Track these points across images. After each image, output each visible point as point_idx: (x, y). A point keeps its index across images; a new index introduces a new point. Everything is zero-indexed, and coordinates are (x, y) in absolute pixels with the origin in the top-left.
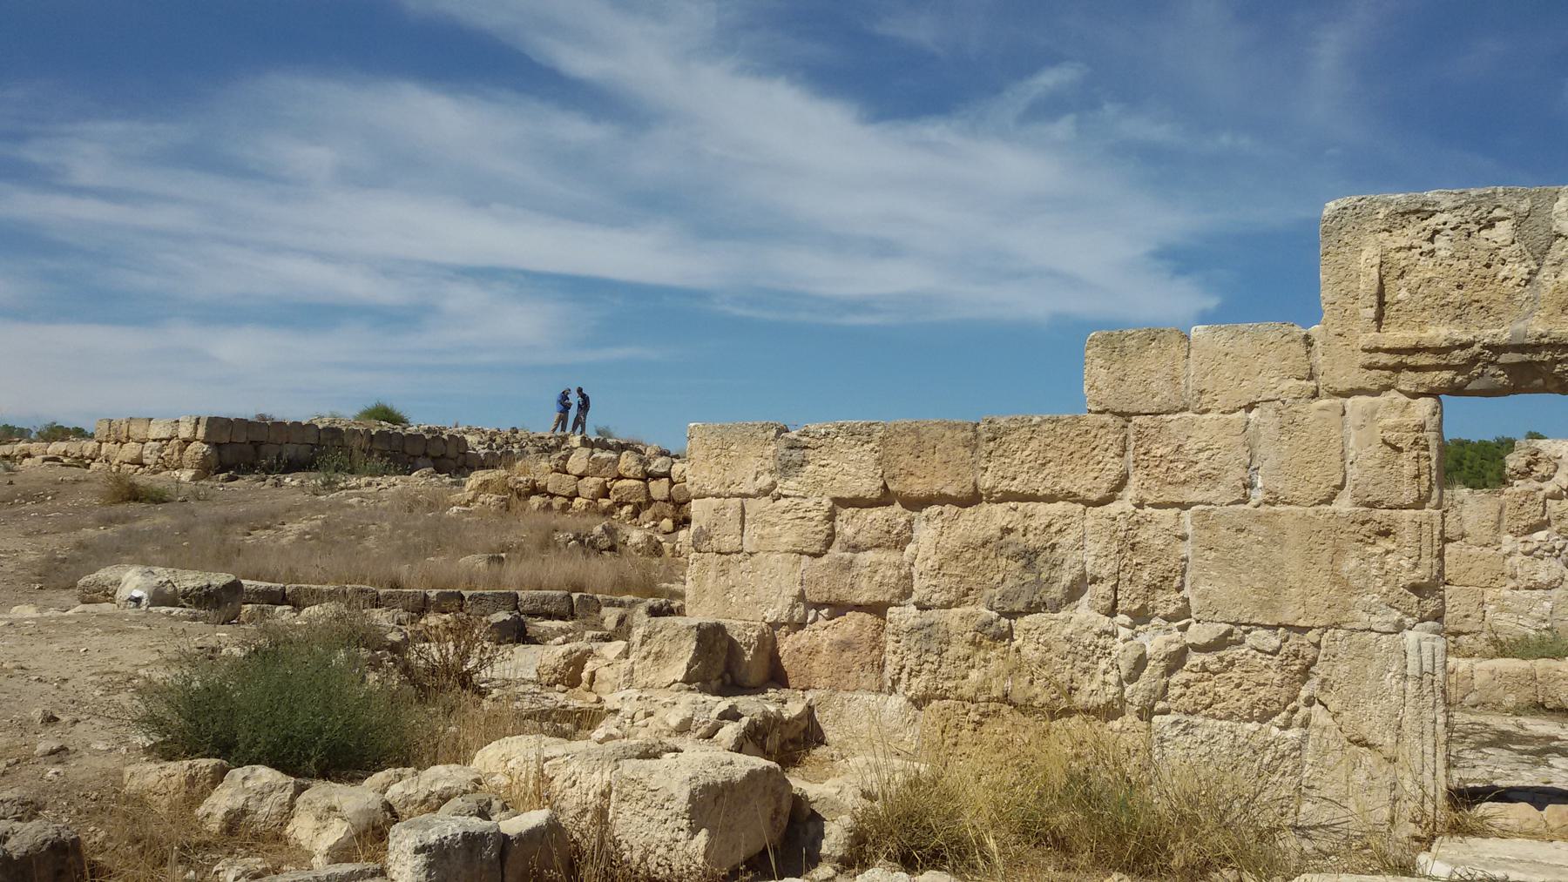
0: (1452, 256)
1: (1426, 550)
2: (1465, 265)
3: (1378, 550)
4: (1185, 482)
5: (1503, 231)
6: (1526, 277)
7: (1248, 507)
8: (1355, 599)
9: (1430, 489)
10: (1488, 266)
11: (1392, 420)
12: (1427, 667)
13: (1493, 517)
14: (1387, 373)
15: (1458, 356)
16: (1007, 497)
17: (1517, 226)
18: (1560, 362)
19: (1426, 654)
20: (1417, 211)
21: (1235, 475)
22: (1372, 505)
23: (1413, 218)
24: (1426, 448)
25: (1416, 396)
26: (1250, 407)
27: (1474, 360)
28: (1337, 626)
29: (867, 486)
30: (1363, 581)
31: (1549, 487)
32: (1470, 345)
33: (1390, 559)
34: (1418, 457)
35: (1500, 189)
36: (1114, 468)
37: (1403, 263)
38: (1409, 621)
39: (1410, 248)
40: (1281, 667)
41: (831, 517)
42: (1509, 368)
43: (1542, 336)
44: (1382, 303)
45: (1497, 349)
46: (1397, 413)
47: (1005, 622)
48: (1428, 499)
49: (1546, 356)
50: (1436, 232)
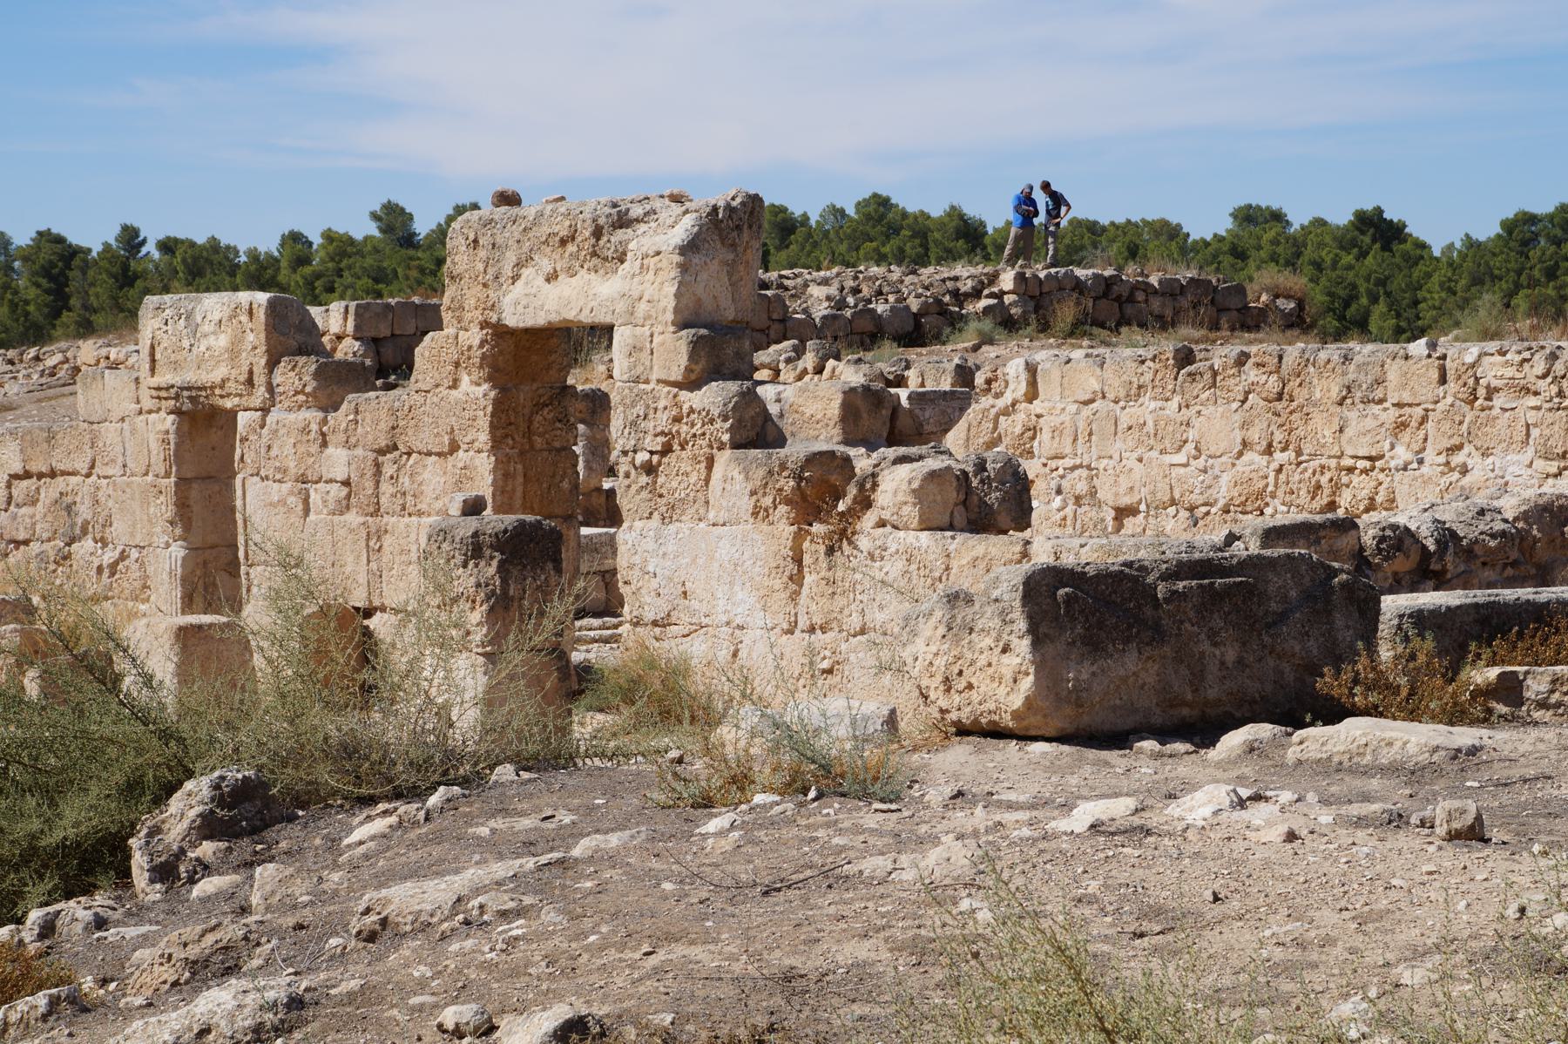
15: (173, 391)
16: (64, 473)
17: (187, 318)
26: (123, 420)
29: (17, 467)
31: (1001, 403)
36: (89, 453)
41: (9, 486)
42: (189, 398)
44: (153, 361)
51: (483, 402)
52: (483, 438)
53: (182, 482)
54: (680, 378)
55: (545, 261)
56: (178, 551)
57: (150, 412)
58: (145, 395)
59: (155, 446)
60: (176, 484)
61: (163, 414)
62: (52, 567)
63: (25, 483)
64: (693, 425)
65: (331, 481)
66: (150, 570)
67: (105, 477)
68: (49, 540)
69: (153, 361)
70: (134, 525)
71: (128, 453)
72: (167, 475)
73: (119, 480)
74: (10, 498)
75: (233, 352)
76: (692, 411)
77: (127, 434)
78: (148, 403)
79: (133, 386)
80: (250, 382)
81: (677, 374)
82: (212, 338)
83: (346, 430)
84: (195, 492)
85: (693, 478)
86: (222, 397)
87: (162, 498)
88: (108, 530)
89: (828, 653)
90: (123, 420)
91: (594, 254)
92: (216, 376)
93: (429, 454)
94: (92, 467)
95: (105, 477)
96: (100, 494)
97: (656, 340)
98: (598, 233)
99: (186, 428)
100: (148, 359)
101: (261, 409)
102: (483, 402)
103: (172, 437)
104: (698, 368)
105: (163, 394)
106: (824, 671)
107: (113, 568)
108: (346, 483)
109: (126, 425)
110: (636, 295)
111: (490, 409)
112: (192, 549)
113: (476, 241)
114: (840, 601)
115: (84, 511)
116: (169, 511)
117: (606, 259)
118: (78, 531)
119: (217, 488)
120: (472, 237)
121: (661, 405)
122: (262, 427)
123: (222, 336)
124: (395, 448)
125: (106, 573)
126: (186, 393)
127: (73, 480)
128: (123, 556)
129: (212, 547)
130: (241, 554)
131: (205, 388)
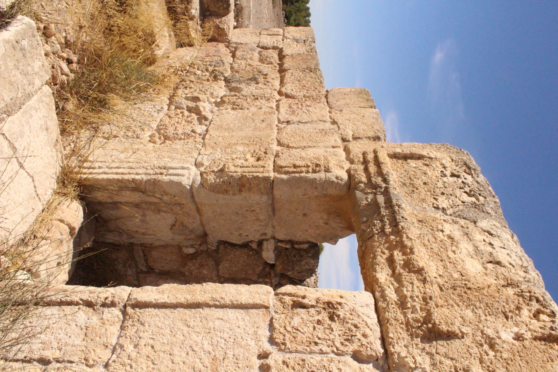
0: (444, 182)
1: (246, 170)
2: (440, 184)
3: (248, 156)
4: (291, 107)
6: (440, 207)
7: (276, 123)
8: (219, 150)
9: (287, 173)
10: (443, 194)
11: (329, 158)
12: (171, 171)
14: (361, 160)
15: (379, 180)
18: (382, 221)
19: (180, 171)
20: (469, 168)
21: (294, 118)
22: (277, 155)
23: (464, 168)
24: (314, 172)
25: (348, 172)
26: (334, 122)
27: (376, 187)
28: (204, 145)
30: (230, 152)
32: (385, 181)
33: (242, 161)
34: (308, 166)
35: (498, 200)
37: (434, 165)
38: (202, 169)
39: (445, 168)
40: (184, 134)
41: (274, 48)
43: (399, 206)
44: (406, 157)
45: (386, 192)
46: (336, 163)
47: (223, 78)
48: (280, 172)
49: (384, 212)
50: (458, 176)
56: (189, 176)
57: (347, 150)
58: (369, 147)
59: (311, 154)
60: (266, 179)
61: (347, 165)
62: (211, 69)
63: (276, 56)
66: (178, 145)
67: (278, 106)
68: (232, 68)
69: (406, 157)
70: (228, 129)
71: (301, 126)
72: (278, 168)
73: (275, 117)
74: (265, 48)
75: (463, 290)
77: (321, 126)
78: (357, 148)
79: (371, 134)
82: (471, 249)
84: (257, 199)
86: (391, 261)
87: (252, 160)
88: (230, 107)
90: (334, 122)
94: (287, 96)
95: (278, 106)
96: (263, 101)
99: (332, 191)
100: (407, 151)
101: (387, 354)
103: (322, 175)
105: (372, 169)
107: (196, 111)
109: (328, 125)
112: (191, 192)
115: (248, 89)
118: (233, 85)
119: (262, 217)
122: (357, 357)
123: (480, 268)
125: (191, 104)
126: (381, 199)
127: (277, 83)
128: (202, 118)
129: (198, 210)
130: (147, 293)
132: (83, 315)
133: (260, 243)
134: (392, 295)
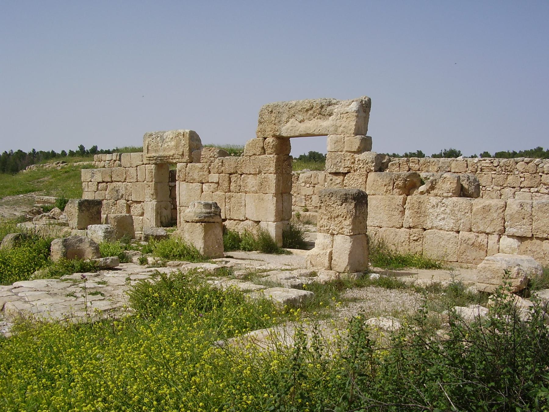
5: (159, 139)
13: (324, 178)
15: (155, 158)
16: (115, 181)
29: (100, 180)
36: (125, 176)
44: (148, 150)
51: (273, 159)
52: (272, 169)
53: (156, 183)
54: (356, 150)
55: (300, 116)
56: (154, 202)
64: (359, 164)
65: (212, 183)
72: (152, 182)
75: (177, 147)
76: (359, 160)
80: (183, 155)
81: (355, 148)
83: (217, 168)
85: (360, 180)
88: (130, 197)
89: (416, 235)
90: (137, 167)
91: (320, 114)
92: (171, 153)
93: (250, 174)
97: (346, 139)
98: (322, 107)
102: (273, 159)
104: (361, 148)
105: (152, 159)
106: (414, 240)
108: (218, 183)
110: (339, 125)
111: (275, 161)
113: (272, 112)
114: (422, 219)
115: (122, 192)
116: (152, 192)
117: (324, 115)
118: (120, 197)
120: (270, 110)
121: (347, 158)
122: (186, 167)
124: (236, 172)
130: (178, 204)
131: (166, 157)
132: (182, 214)
133: (170, 186)
134: (177, 160)
